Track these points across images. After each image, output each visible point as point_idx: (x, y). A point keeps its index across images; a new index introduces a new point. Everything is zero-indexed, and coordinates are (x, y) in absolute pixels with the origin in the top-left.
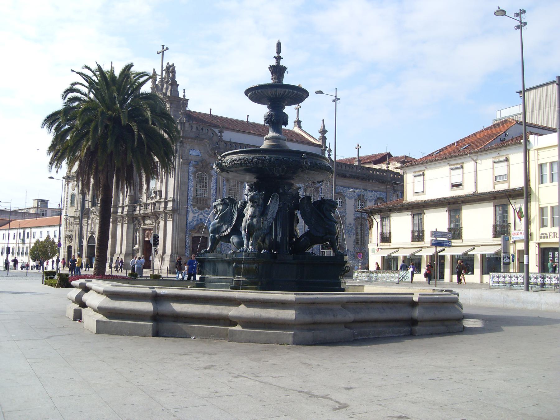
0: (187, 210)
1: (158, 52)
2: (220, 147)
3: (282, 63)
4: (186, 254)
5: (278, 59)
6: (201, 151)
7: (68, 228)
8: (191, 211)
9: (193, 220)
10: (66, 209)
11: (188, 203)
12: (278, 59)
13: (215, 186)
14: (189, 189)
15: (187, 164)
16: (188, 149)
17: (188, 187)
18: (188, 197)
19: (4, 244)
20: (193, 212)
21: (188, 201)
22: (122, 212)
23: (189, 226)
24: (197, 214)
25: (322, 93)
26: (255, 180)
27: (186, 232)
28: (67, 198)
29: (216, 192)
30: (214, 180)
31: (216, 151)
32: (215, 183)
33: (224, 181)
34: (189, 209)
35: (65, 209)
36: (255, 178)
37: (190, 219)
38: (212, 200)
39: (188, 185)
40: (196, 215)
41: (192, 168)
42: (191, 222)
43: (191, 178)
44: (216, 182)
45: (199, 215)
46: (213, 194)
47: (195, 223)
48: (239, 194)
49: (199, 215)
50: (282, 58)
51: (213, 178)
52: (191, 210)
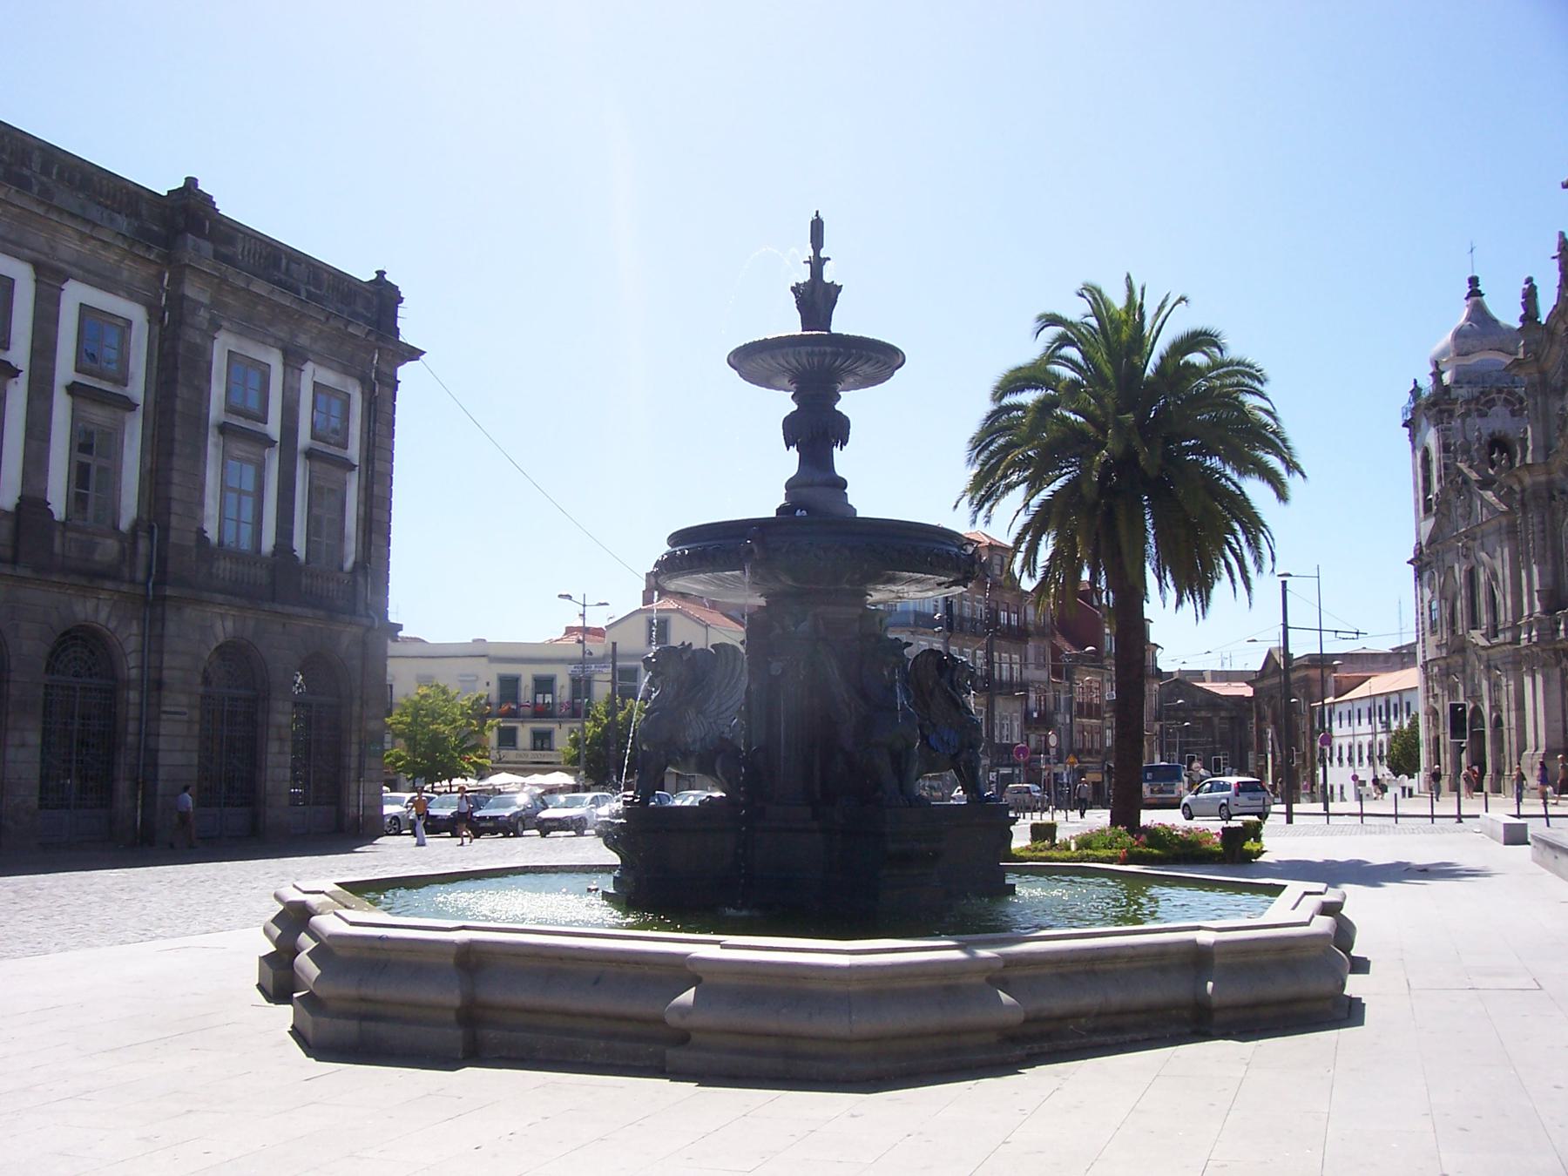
1: (1562, 184)
3: (827, 277)
5: (817, 264)
7: (1431, 690)
10: (1424, 641)
12: (817, 264)
19: (1358, 735)
22: (1530, 639)
26: (762, 602)
28: (1422, 614)
36: (761, 596)
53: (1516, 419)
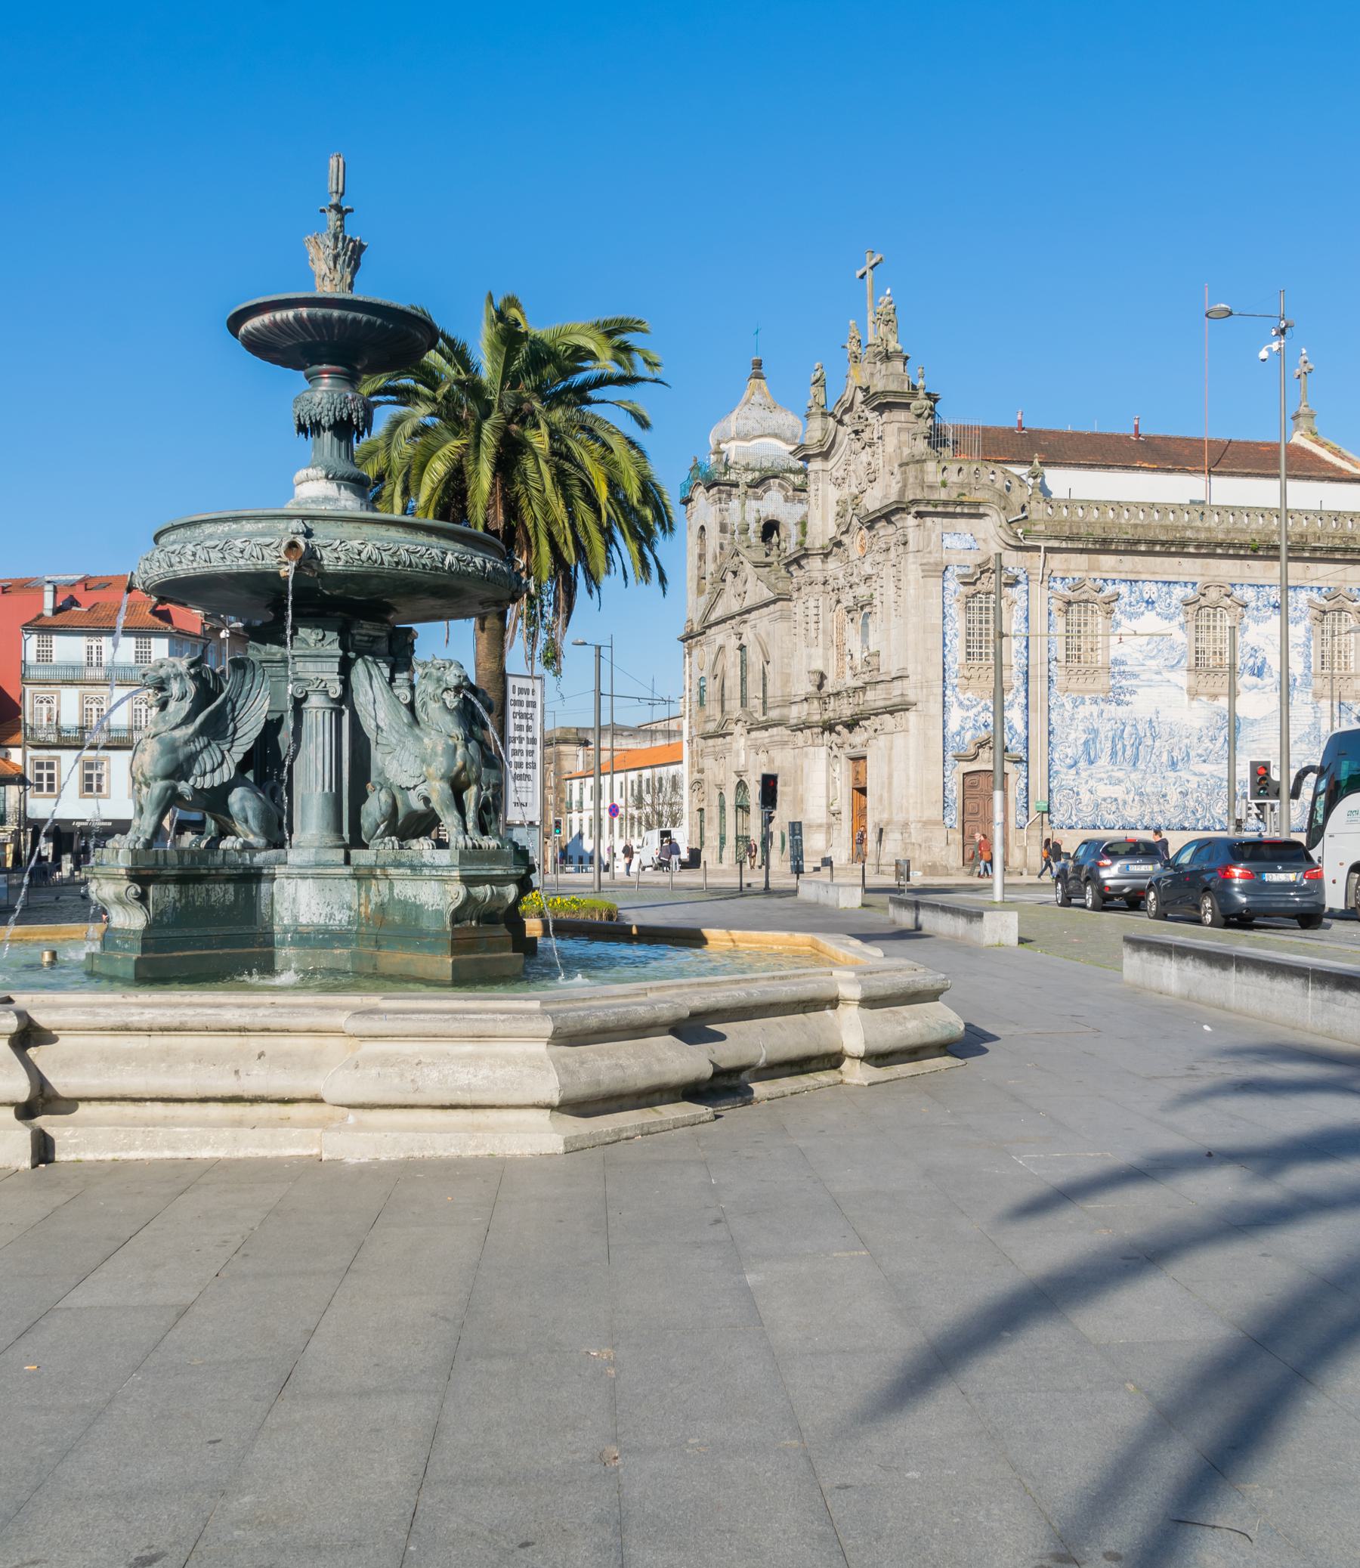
0: (944, 702)
2: (1033, 516)
4: (947, 819)
6: (977, 536)
8: (956, 705)
9: (963, 728)
11: (944, 681)
13: (1024, 630)
14: (947, 642)
15: (939, 577)
16: (937, 532)
17: (944, 638)
18: (944, 664)
20: (961, 704)
21: (944, 677)
23: (950, 743)
24: (975, 711)
25: (1231, 314)
27: (944, 761)
29: (1027, 647)
30: (1020, 613)
31: (1020, 531)
32: (1023, 620)
33: (1050, 614)
34: (950, 698)
35: (687, 716)
37: (953, 726)
38: (1015, 669)
39: (944, 634)
40: (971, 713)
41: (952, 585)
42: (959, 734)
43: (955, 611)
44: (1027, 619)
45: (979, 713)
46: (1017, 652)
47: (968, 736)
48: (1100, 645)
49: (979, 713)
50: (351, 211)
51: (1016, 607)
52: (955, 700)
53: (789, 504)
